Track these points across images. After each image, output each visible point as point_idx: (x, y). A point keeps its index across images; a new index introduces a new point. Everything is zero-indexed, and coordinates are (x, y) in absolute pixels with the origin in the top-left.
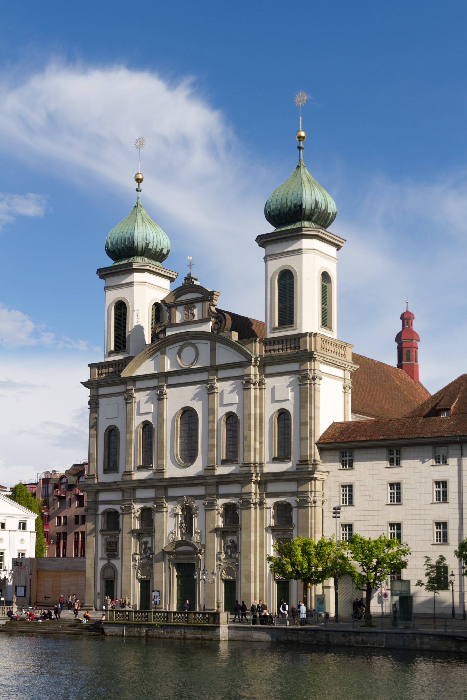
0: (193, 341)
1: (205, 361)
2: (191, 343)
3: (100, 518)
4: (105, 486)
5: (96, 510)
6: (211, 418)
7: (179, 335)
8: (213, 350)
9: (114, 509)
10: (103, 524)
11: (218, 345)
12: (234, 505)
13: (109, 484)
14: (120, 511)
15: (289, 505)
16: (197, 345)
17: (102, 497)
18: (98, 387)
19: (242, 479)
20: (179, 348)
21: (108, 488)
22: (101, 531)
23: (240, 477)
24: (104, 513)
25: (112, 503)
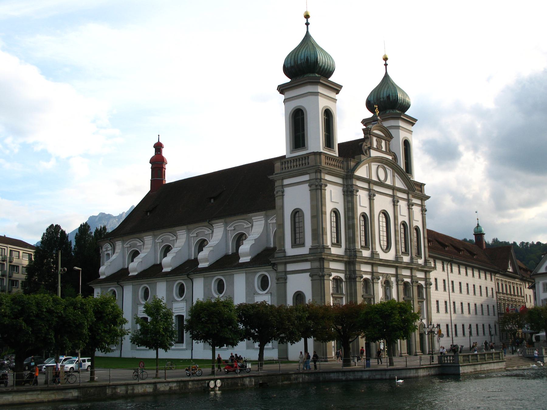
0: (386, 166)
1: (389, 182)
2: (384, 167)
3: (331, 282)
4: (339, 257)
5: (330, 275)
6: (396, 221)
7: (383, 158)
8: (394, 176)
9: (339, 277)
10: (333, 290)
11: (396, 174)
12: (408, 282)
13: (338, 256)
14: (344, 280)
15: (421, 285)
16: (386, 169)
17: (333, 265)
18: (326, 174)
19: (415, 267)
20: (376, 166)
21: (341, 259)
22: (332, 294)
23: (415, 265)
24: (333, 278)
25: (338, 271)
